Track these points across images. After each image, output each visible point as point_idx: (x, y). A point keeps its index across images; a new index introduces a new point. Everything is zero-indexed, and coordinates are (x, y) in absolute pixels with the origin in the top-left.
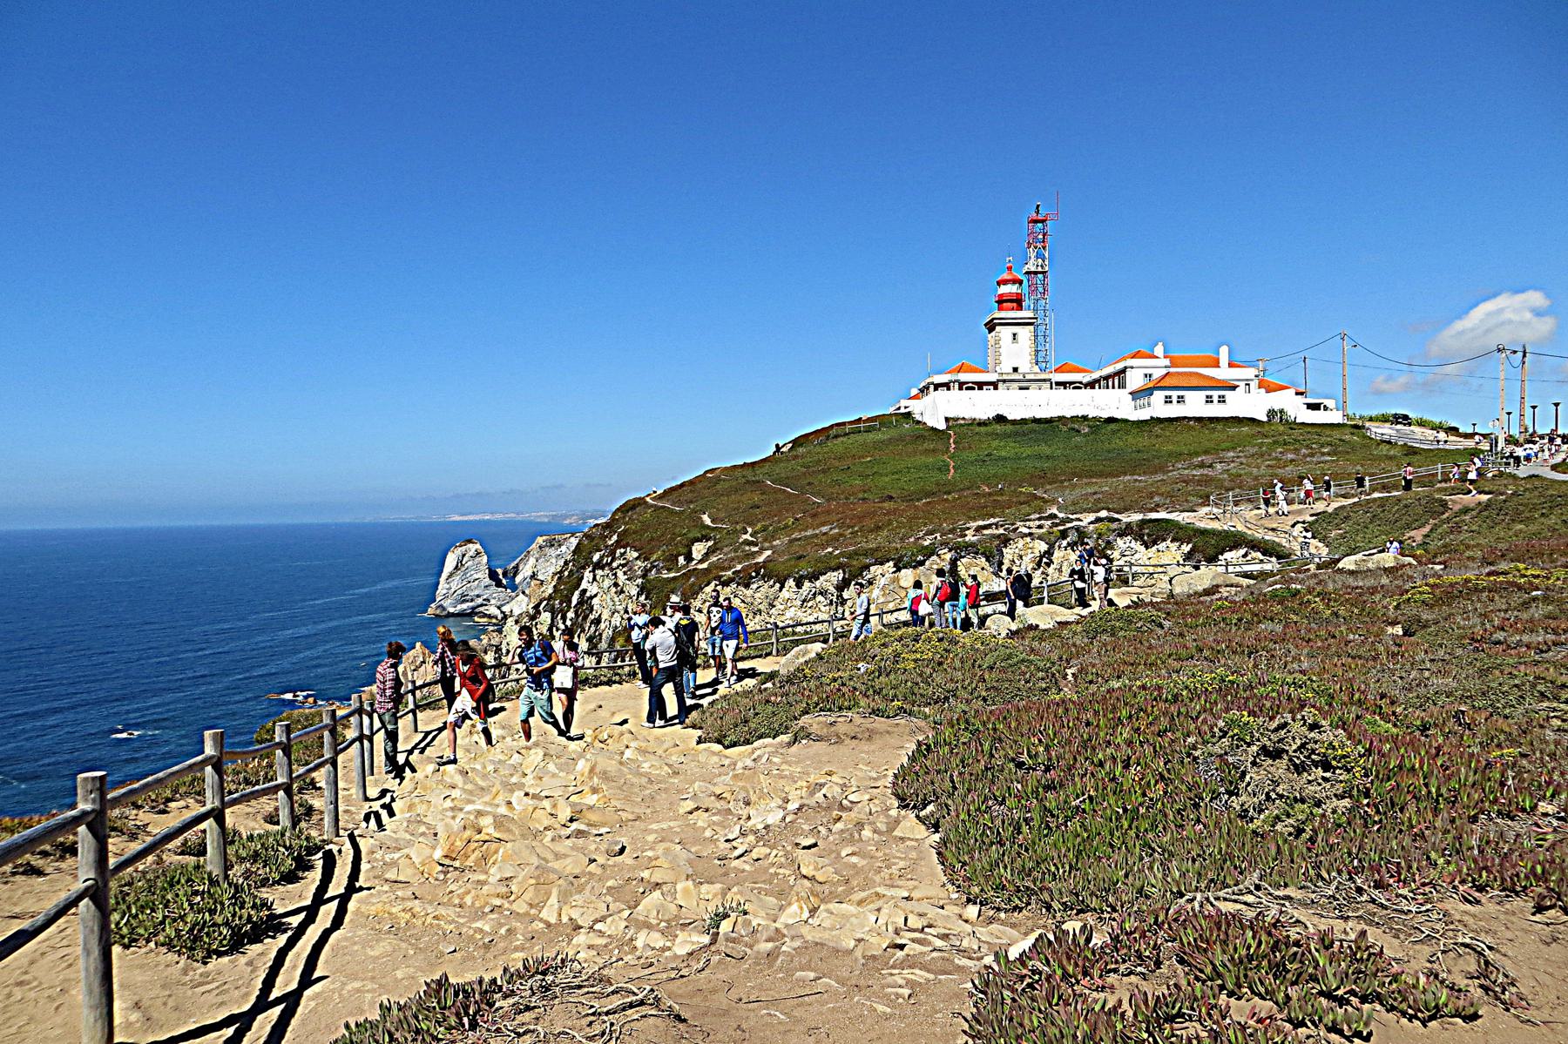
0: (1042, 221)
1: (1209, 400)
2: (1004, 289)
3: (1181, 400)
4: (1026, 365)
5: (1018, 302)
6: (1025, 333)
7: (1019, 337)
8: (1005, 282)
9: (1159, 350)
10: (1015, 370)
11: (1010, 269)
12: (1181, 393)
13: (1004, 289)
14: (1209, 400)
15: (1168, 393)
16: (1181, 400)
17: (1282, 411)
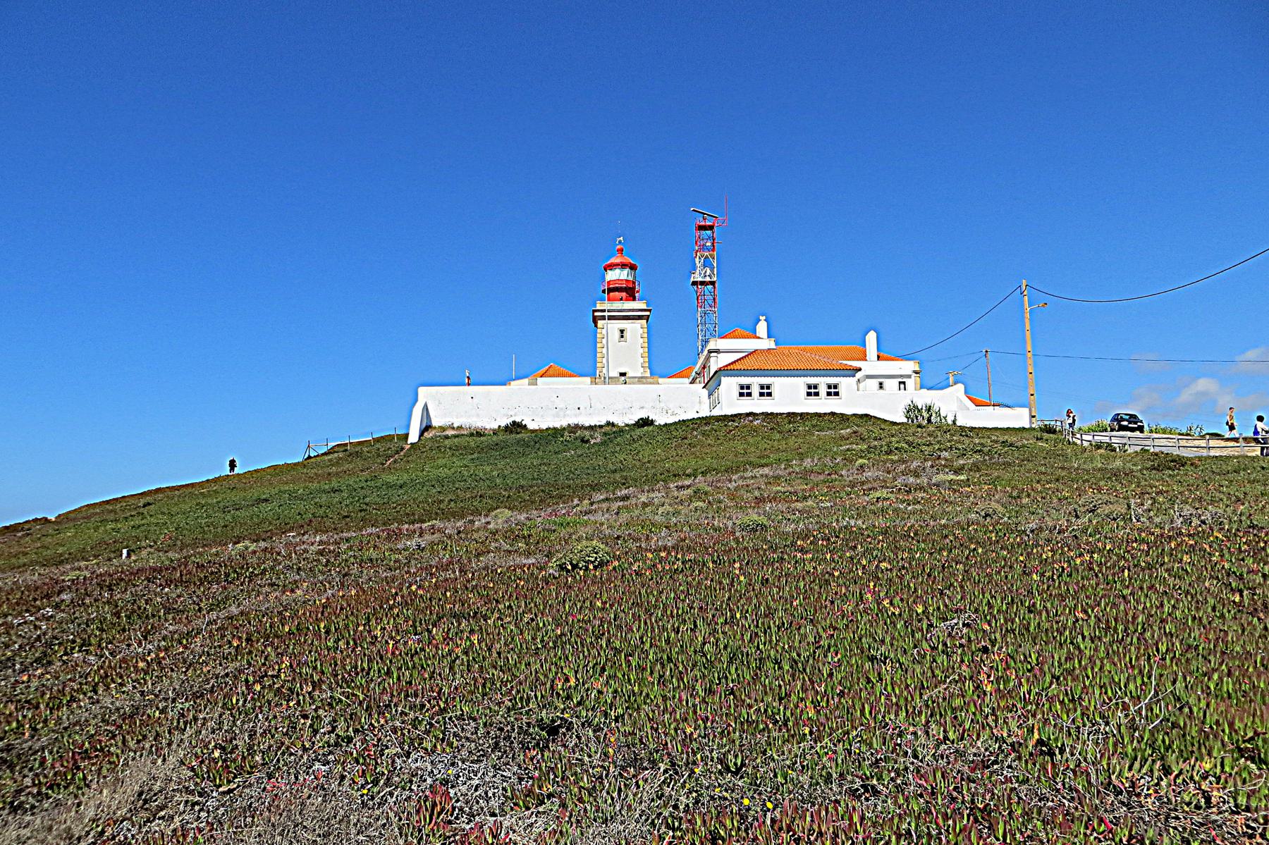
0: (711, 228)
1: (812, 391)
2: (613, 275)
3: (766, 392)
4: (636, 371)
5: (629, 291)
6: (636, 329)
7: (627, 334)
8: (611, 267)
9: (762, 328)
10: (623, 374)
11: (621, 251)
12: (765, 381)
13: (613, 275)
14: (812, 391)
15: (745, 380)
16: (766, 392)
17: (929, 409)
